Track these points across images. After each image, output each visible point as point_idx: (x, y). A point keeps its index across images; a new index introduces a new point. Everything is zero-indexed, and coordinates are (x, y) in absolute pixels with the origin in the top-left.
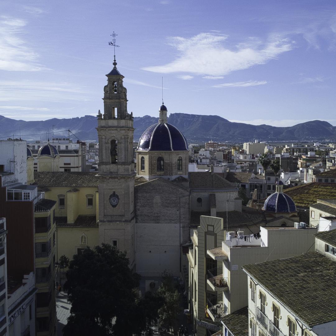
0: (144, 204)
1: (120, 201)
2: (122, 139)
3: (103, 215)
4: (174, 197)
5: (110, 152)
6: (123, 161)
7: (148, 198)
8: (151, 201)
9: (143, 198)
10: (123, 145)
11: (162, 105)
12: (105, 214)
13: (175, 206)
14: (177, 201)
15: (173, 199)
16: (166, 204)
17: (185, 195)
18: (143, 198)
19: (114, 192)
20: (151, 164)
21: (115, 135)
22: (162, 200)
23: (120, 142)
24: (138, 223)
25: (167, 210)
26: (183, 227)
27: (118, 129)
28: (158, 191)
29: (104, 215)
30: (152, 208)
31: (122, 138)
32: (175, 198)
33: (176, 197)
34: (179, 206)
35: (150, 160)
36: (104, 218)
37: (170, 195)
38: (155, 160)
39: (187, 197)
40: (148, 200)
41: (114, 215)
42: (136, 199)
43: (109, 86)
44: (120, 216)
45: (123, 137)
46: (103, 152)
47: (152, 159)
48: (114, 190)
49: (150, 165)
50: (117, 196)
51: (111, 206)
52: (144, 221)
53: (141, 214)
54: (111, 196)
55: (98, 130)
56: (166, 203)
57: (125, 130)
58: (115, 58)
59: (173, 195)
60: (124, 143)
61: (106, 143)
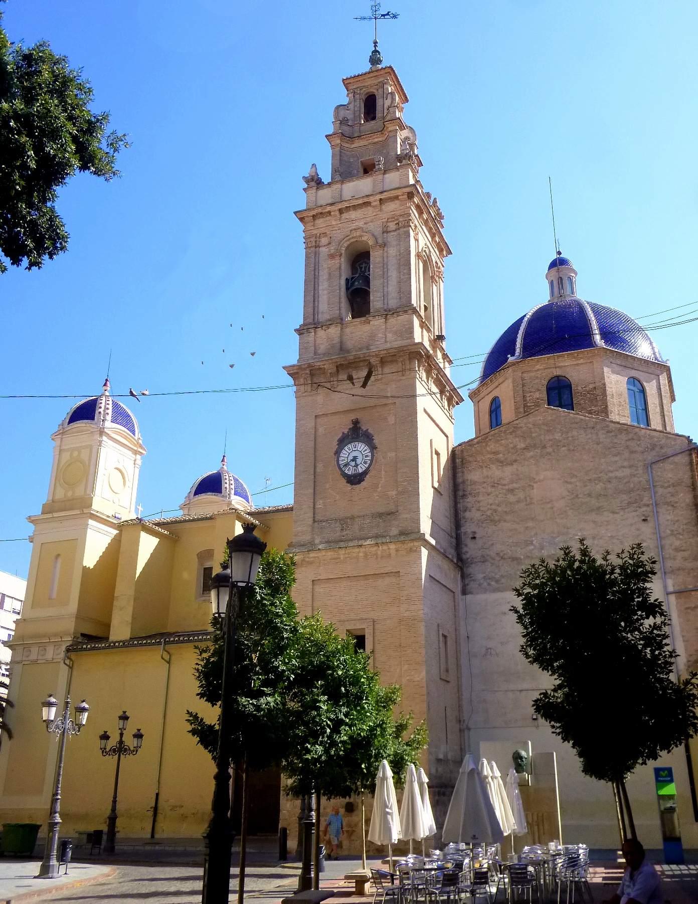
0: (495, 511)
1: (379, 455)
2: (387, 232)
3: (310, 521)
4: (624, 467)
5: (343, 282)
6: (393, 303)
7: (511, 486)
8: (521, 495)
9: (490, 490)
10: (392, 251)
11: (555, 256)
12: (318, 518)
13: (629, 503)
14: (636, 479)
15: (619, 474)
16: (587, 499)
17: (670, 452)
18: (490, 490)
19: (356, 423)
20: (525, 406)
21: (361, 224)
22: (570, 486)
23: (380, 241)
24: (471, 593)
25: (594, 522)
26: (679, 593)
27: (371, 199)
28: (549, 450)
29: (314, 521)
30: (530, 524)
31: (389, 229)
32: (627, 472)
33: (630, 467)
34: (646, 500)
35: (521, 392)
36: (313, 530)
37: (603, 460)
38: (538, 390)
39: (677, 459)
40: (511, 491)
41: (352, 518)
42: (460, 493)
43: (351, 106)
44: (380, 515)
45: (392, 226)
46: (320, 288)
47: (526, 388)
48: (353, 416)
49: (522, 410)
50: (368, 439)
51: (344, 481)
52: (497, 581)
53: (483, 556)
54: (343, 442)
55: (302, 219)
56: (589, 495)
57: (397, 198)
58: (375, 46)
59: (616, 459)
60: (394, 243)
61: (332, 256)
